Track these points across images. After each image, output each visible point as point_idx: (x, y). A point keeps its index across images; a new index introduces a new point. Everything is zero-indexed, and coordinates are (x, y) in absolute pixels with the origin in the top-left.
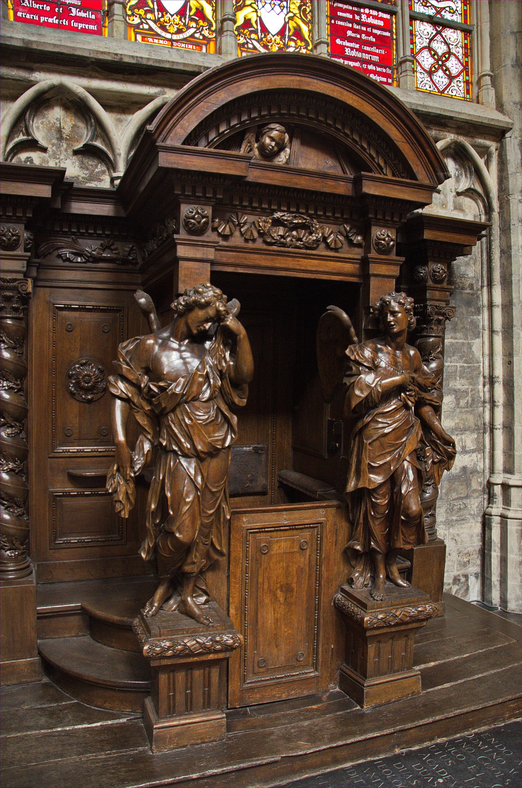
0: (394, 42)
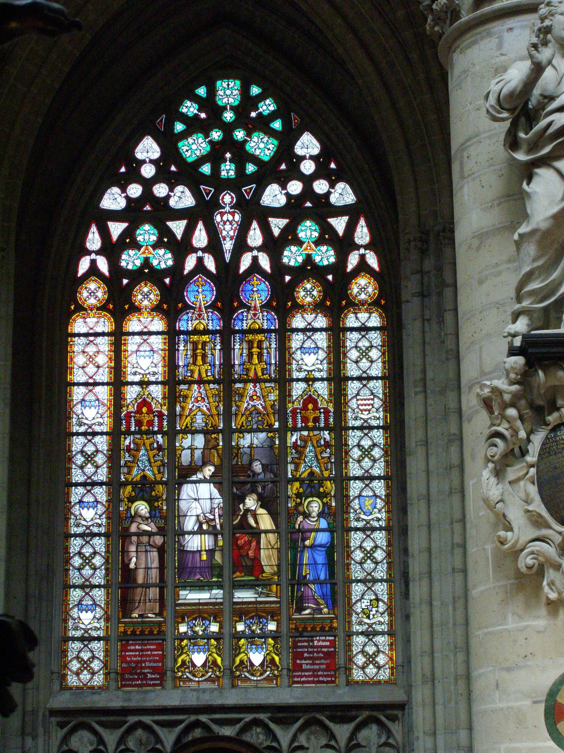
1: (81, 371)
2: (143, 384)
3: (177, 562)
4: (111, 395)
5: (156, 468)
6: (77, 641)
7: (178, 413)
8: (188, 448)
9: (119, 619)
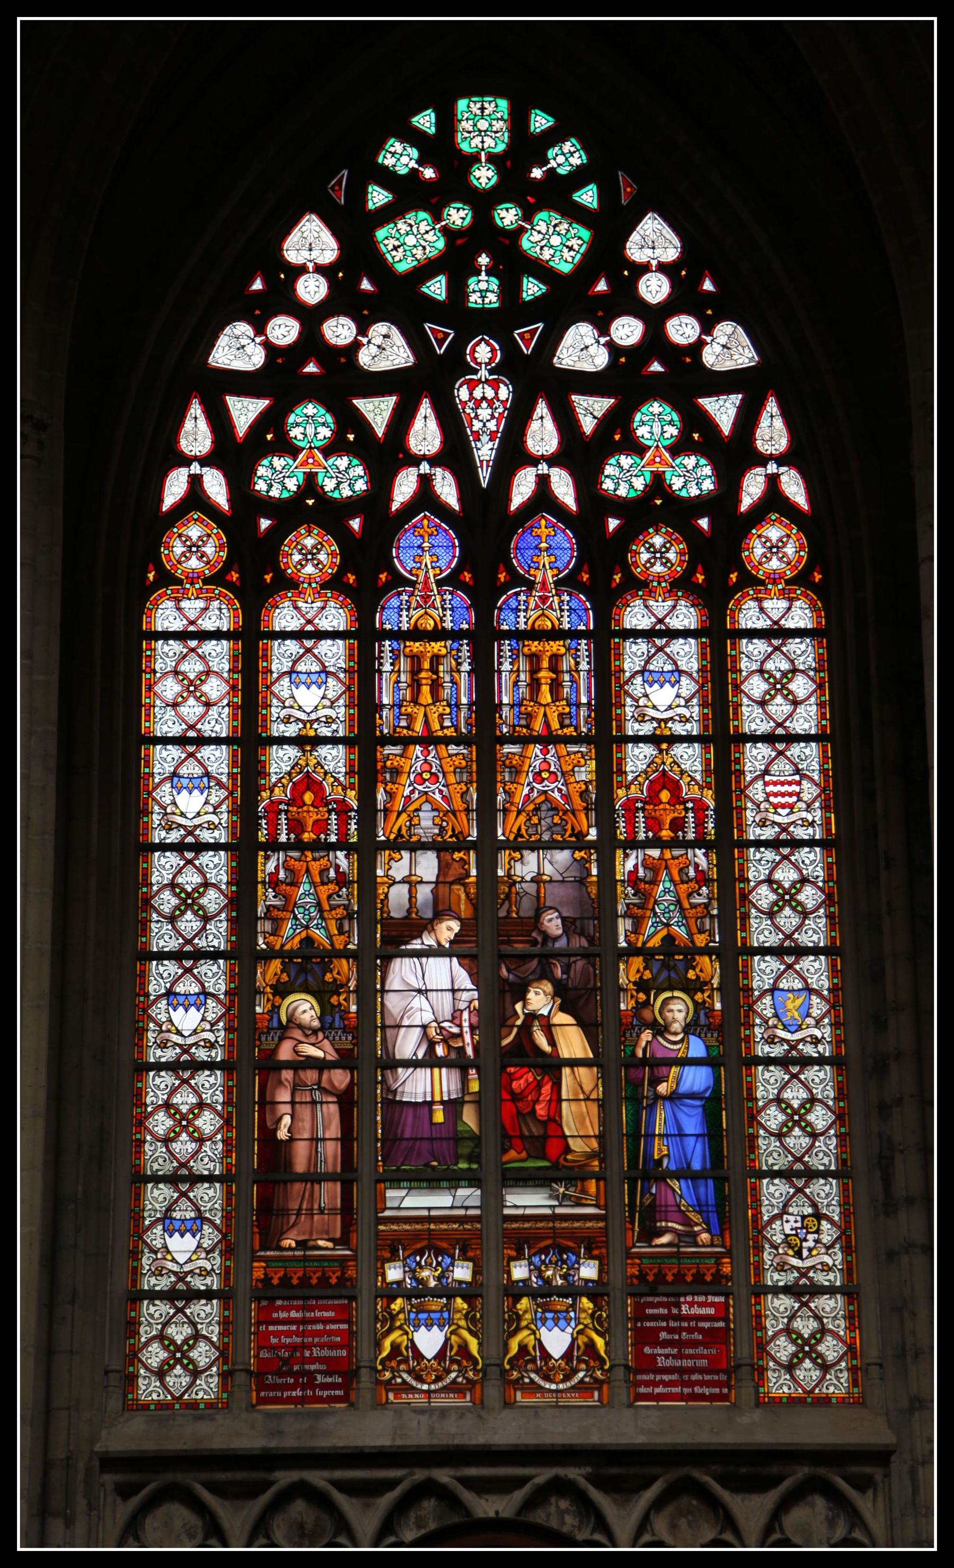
0: (732, 1333)
1: (170, 712)
2: (305, 742)
3: (380, 1126)
4: (234, 764)
5: (333, 922)
6: (161, 1299)
7: (380, 806)
8: (403, 881)
9: (253, 1252)
